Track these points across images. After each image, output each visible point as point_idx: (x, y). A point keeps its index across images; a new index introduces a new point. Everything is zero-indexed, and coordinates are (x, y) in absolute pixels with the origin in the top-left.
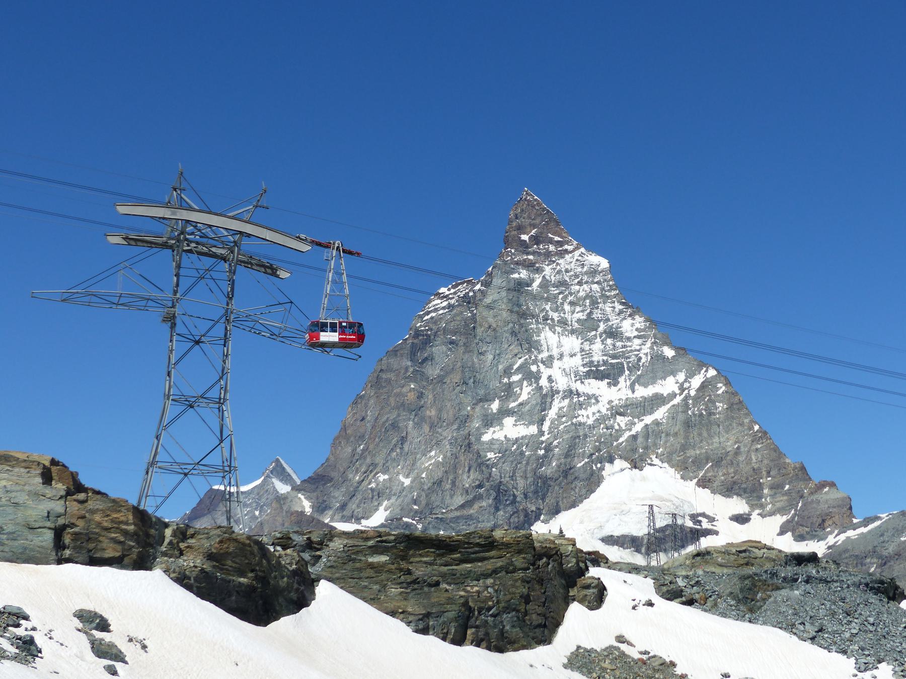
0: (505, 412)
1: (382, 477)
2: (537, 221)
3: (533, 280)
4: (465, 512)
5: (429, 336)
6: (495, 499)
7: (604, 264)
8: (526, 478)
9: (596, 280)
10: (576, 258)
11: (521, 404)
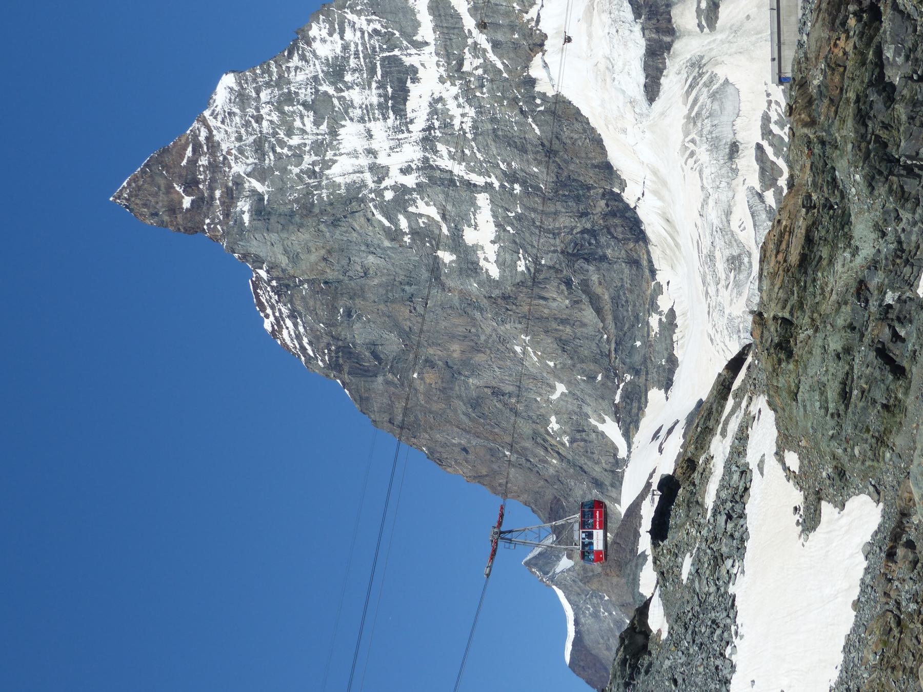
0: (456, 243)
1: (554, 425)
2: (162, 182)
3: (254, 192)
4: (607, 307)
5: (338, 348)
6: (587, 260)
7: (228, 80)
8: (556, 213)
9: (254, 94)
10: (219, 124)
11: (444, 217)
